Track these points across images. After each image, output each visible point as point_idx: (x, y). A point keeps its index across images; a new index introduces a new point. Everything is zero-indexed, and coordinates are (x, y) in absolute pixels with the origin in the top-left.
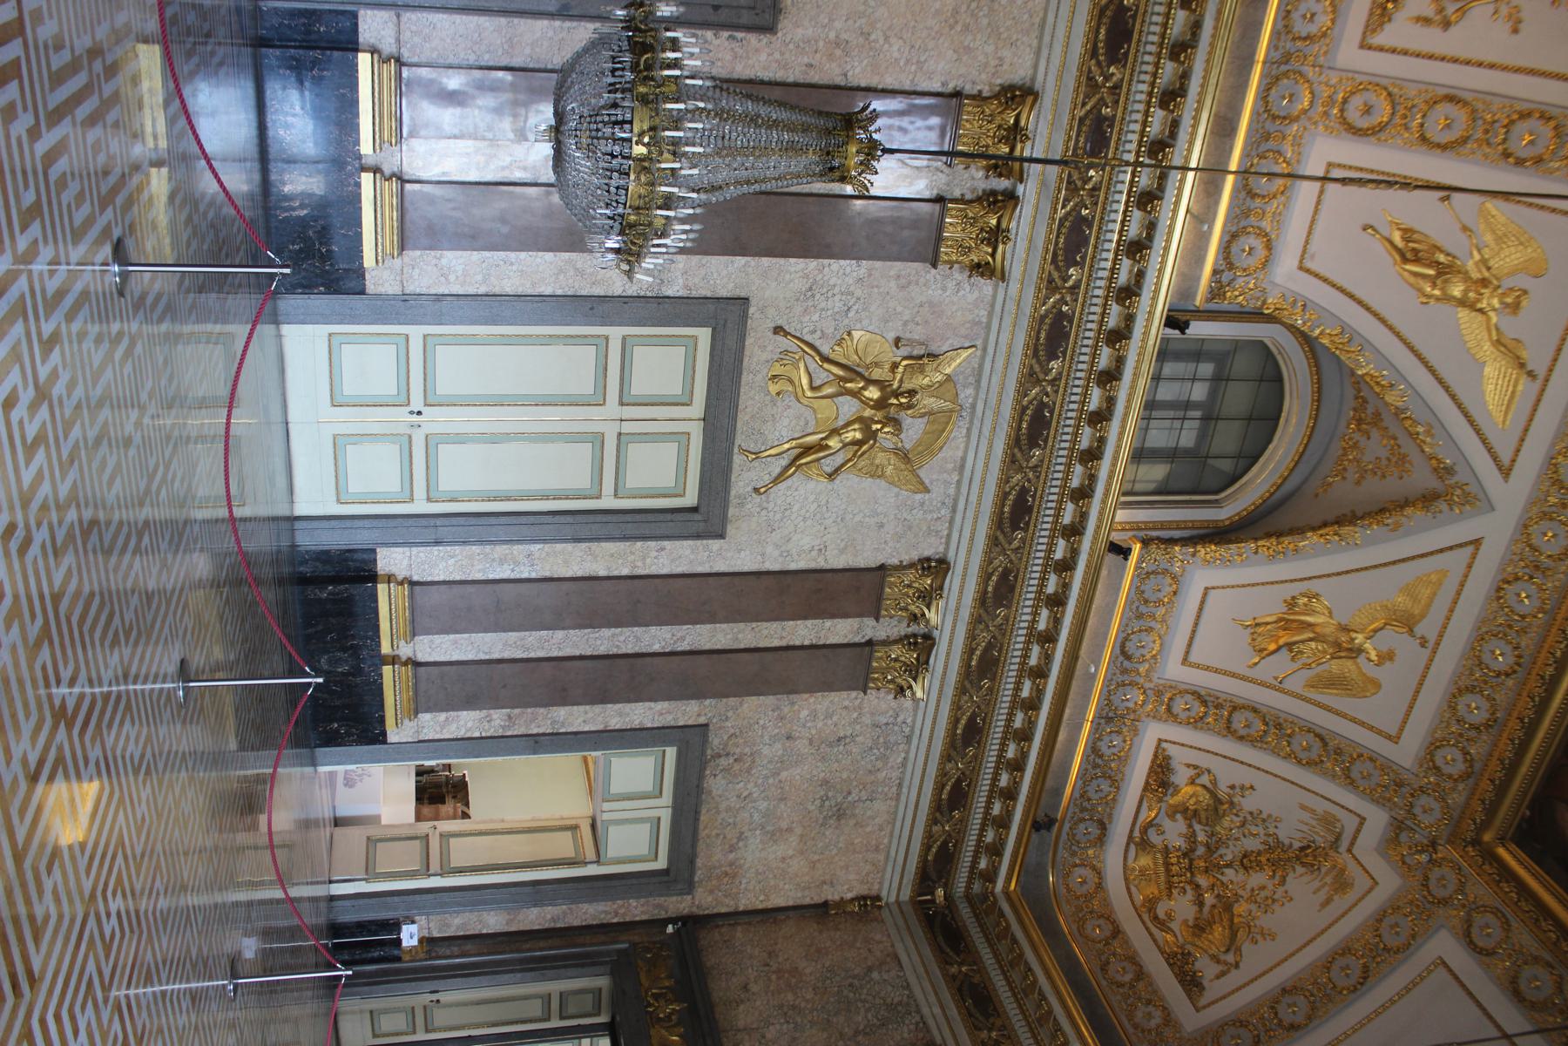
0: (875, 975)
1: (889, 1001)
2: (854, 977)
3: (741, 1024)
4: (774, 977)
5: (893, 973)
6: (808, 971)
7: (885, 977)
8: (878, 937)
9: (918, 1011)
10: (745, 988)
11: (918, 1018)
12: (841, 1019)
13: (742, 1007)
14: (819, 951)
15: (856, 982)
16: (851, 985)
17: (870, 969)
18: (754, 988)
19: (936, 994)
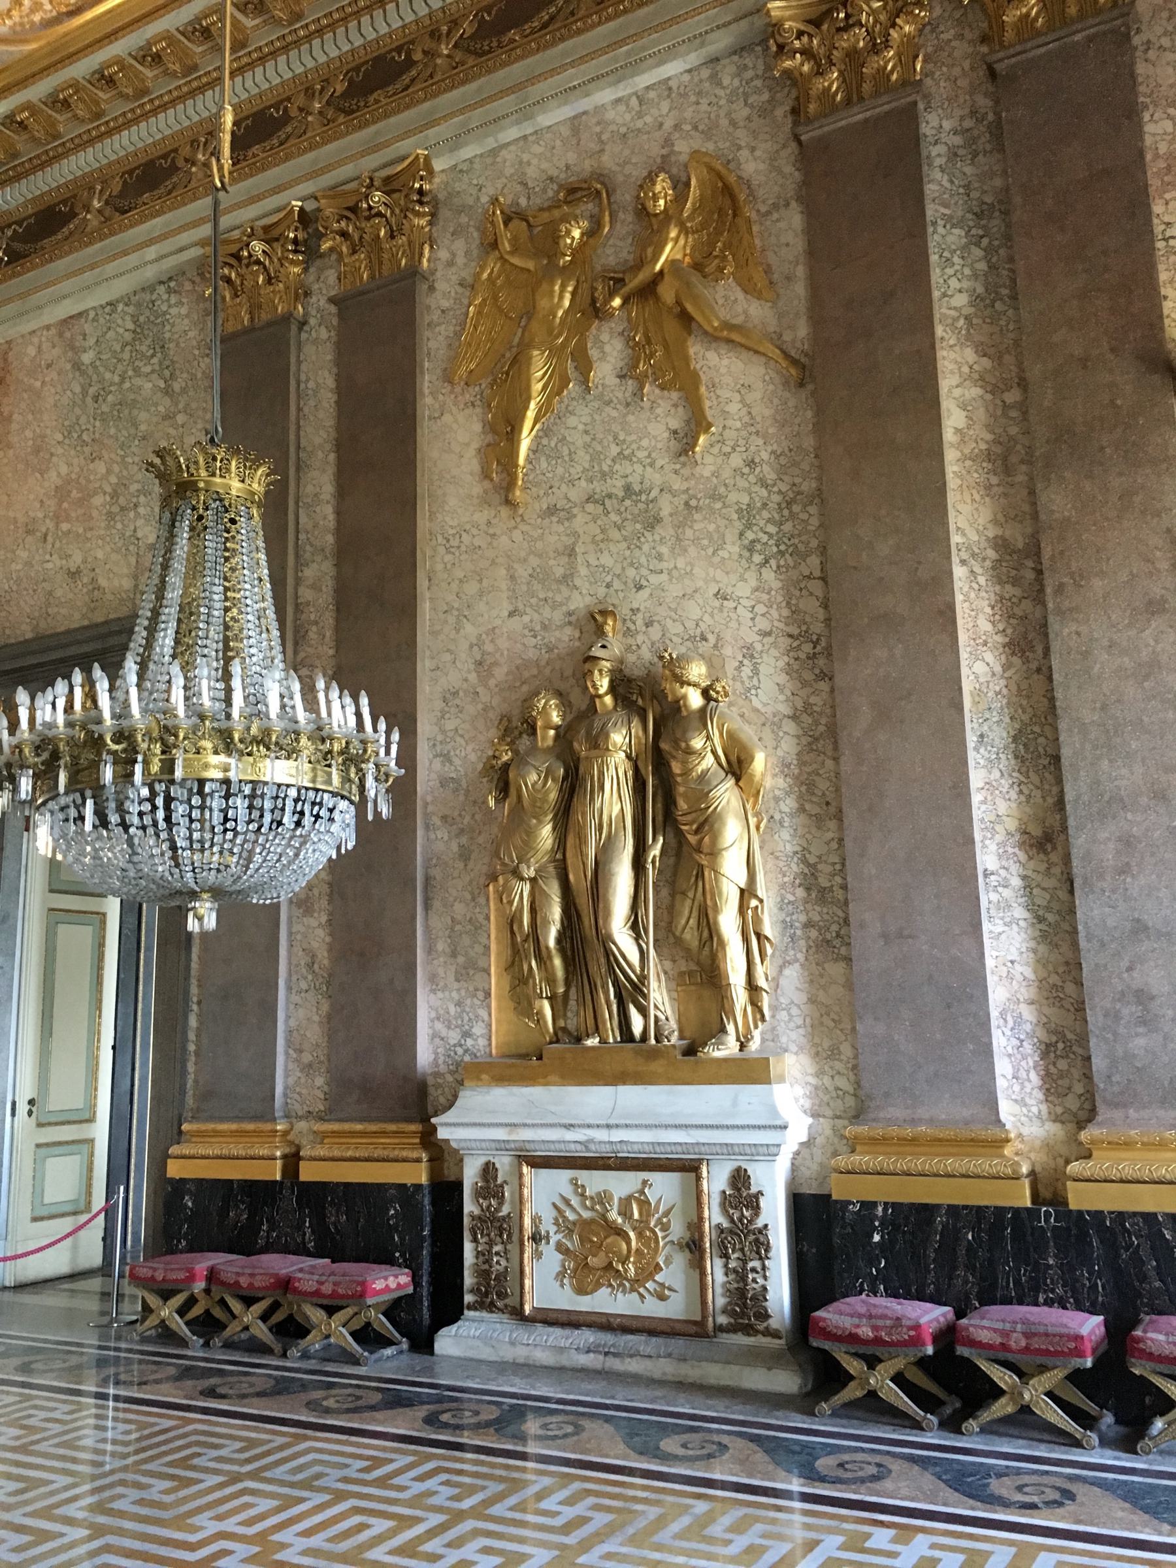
0: (87, 358)
1: (128, 336)
2: (85, 393)
3: (127, 584)
4: (65, 526)
5: (88, 327)
6: (64, 470)
7: (91, 341)
8: (32, 351)
9: (151, 288)
10: (74, 575)
11: (161, 289)
12: (143, 416)
13: (103, 582)
14: (37, 450)
15: (92, 391)
16: (96, 399)
17: (77, 366)
18: (77, 559)
19: (125, 253)
